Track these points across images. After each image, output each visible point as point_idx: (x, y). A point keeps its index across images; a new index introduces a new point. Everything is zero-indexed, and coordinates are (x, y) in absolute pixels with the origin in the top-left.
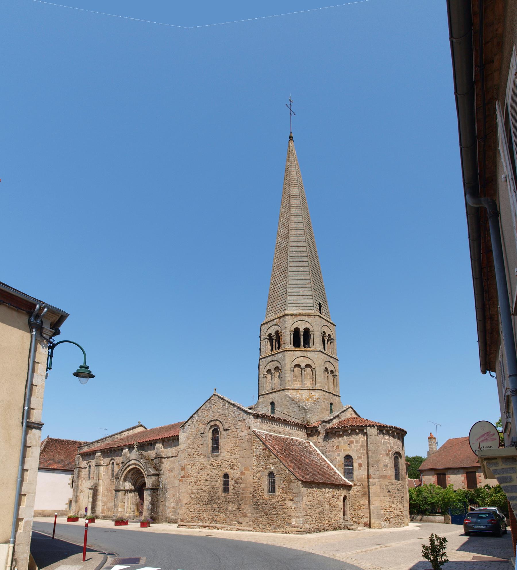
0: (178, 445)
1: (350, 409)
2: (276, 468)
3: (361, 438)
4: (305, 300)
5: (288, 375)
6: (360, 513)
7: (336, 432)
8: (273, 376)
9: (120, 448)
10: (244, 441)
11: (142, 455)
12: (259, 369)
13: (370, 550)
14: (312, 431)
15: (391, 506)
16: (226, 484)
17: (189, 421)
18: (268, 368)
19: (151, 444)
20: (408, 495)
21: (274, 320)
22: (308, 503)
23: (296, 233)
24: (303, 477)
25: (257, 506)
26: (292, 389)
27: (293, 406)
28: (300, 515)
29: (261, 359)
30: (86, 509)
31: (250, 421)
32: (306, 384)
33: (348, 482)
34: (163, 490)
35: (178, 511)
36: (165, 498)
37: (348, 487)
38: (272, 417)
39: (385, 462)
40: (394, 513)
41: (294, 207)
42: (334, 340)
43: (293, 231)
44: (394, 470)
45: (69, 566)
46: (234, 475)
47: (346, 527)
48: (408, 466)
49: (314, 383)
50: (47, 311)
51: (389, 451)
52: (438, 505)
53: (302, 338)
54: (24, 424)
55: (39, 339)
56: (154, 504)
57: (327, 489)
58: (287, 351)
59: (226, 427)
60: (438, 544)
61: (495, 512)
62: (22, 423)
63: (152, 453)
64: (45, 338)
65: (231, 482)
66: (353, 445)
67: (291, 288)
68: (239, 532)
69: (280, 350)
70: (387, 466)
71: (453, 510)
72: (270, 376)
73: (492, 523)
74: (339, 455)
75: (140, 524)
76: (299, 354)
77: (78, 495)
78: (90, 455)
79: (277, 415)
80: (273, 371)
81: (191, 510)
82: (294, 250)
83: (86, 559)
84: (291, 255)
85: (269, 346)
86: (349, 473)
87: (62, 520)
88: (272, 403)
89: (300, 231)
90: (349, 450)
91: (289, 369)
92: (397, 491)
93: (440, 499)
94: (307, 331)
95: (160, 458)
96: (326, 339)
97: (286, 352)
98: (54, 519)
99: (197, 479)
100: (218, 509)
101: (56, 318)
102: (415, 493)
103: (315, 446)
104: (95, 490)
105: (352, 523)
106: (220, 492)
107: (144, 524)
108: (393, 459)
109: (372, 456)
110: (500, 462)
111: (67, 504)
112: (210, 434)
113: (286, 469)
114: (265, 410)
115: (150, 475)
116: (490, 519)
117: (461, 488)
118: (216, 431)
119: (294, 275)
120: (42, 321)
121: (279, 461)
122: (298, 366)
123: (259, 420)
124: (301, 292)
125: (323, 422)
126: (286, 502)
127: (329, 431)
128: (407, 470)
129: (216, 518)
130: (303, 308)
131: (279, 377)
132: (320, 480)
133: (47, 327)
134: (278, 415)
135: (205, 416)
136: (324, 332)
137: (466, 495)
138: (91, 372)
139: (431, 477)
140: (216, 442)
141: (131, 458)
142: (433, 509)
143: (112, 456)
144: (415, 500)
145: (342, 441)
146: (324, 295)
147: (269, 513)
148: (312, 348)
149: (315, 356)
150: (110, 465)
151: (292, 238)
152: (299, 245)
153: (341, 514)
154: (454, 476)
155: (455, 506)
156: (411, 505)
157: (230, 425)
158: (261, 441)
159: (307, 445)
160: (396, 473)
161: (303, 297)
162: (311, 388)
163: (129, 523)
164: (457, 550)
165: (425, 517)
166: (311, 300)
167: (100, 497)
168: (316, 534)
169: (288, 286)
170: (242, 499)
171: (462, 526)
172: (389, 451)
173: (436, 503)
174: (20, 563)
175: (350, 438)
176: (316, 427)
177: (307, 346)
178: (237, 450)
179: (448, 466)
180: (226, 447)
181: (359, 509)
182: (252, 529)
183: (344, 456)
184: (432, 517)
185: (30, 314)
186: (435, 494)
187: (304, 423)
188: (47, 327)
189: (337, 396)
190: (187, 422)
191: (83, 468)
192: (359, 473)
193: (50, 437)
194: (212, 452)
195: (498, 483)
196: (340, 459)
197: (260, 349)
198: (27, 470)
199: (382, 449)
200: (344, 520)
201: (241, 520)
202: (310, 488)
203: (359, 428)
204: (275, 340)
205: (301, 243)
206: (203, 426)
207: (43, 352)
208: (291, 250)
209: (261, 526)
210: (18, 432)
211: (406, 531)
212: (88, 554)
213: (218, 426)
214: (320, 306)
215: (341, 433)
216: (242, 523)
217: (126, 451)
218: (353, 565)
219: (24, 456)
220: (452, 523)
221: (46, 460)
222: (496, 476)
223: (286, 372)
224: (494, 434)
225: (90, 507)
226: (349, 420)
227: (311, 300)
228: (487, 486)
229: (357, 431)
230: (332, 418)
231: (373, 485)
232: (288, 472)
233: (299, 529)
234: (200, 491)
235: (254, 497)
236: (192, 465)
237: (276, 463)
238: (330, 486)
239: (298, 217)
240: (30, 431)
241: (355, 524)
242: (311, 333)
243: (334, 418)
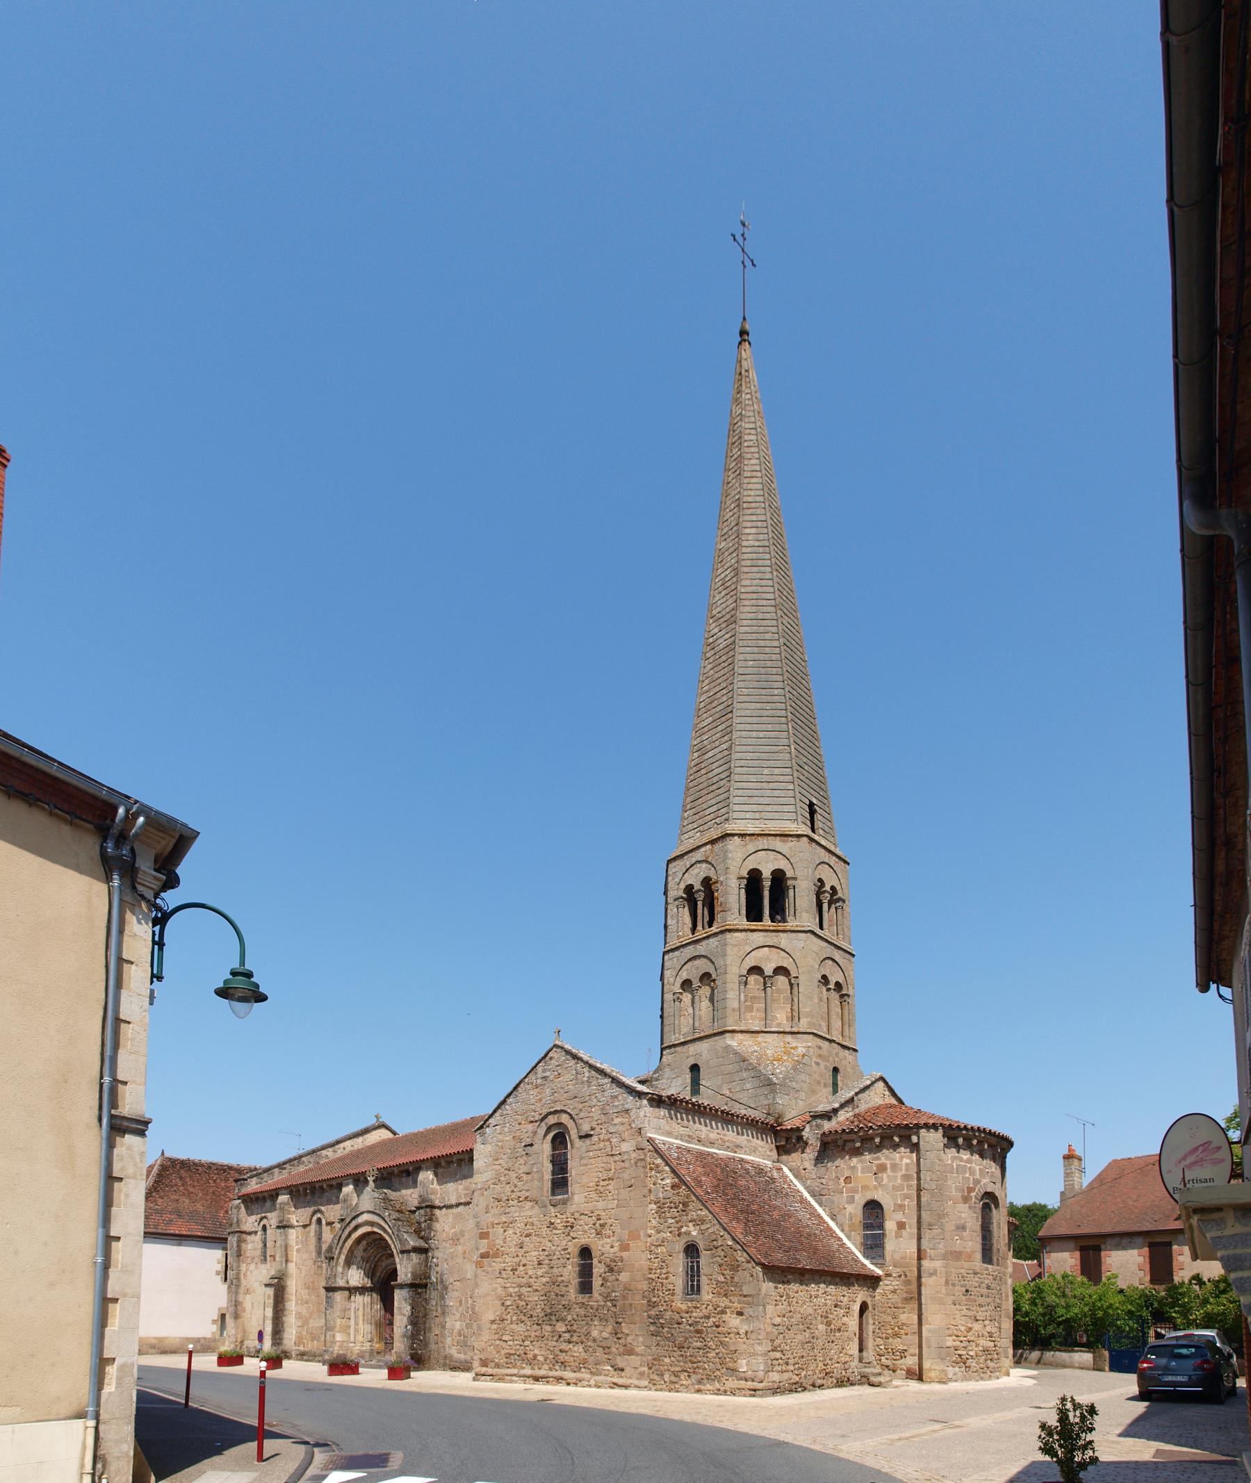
0: (471, 1176)
1: (881, 1084)
2: (702, 1232)
3: (904, 1158)
4: (776, 793)
5: (732, 995)
6: (897, 1344)
7: (845, 1141)
8: (697, 998)
9: (334, 1183)
10: (627, 1164)
11: (386, 1200)
12: (662, 979)
13: (920, 1435)
14: (788, 1139)
15: (971, 1329)
16: (586, 1272)
17: (497, 1114)
18: (684, 975)
19: (408, 1173)
20: (1011, 1300)
21: (699, 847)
22: (778, 1320)
23: (754, 609)
24: (766, 1255)
25: (658, 1326)
26: (742, 1032)
28: (759, 1349)
29: (668, 952)
30: (261, 1335)
31: (642, 1114)
32: (774, 1018)
33: (872, 1267)
34: (439, 1287)
35: (472, 1341)
36: (444, 1306)
37: (872, 1282)
38: (693, 1104)
39: (960, 1217)
40: (977, 1345)
41: (752, 536)
42: (844, 901)
43: (747, 603)
44: (979, 1239)
45: (229, 1473)
46: (604, 1250)
47: (864, 1380)
48: (1012, 1228)
49: (794, 1016)
50: (146, 823)
51: (970, 1190)
52: (1080, 1326)
53: (767, 897)
54: (105, 1121)
55: (128, 898)
56: (418, 1323)
57: (822, 1286)
58: (730, 931)
59: (585, 1128)
60: (1077, 1420)
61: (1210, 1343)
62: (100, 1119)
63: (410, 1196)
64: (142, 896)
65: (598, 1269)
66: (883, 1176)
67: (742, 763)
68: (617, 1392)
69: (714, 929)
70: (963, 1228)
71: (1110, 1337)
72: (690, 996)
73: (1203, 1369)
74: (851, 1200)
75: (386, 1371)
76: (758, 938)
77: (241, 1299)
78: (264, 1199)
79: (704, 1099)
80: (696, 983)
81: (505, 1338)
82: (749, 657)
83: (265, 1456)
84: (741, 671)
85: (687, 919)
86: (874, 1246)
87: (206, 1363)
88: (695, 1068)
89: (764, 603)
90: (875, 1188)
91: (736, 979)
92: (985, 1291)
93: (1086, 1309)
94: (779, 878)
95: (429, 1207)
96: (826, 898)
97: (728, 935)
98: (187, 1358)
99: (517, 1260)
100: (567, 1336)
101: (167, 844)
102: (1028, 1296)
103: (796, 1177)
104: (279, 1288)
105: (878, 1370)
106: (572, 1293)
107: (396, 1372)
108: (979, 1211)
109: (929, 1204)
110: (1230, 1217)
111: (214, 1322)
112: (547, 1147)
113: (727, 1236)
114: (677, 1086)
115: (408, 1252)
116: (1199, 1361)
117: (1137, 1284)
118: (560, 1140)
119: (749, 727)
120: (132, 850)
121: (710, 1217)
122: (756, 970)
123: (663, 1112)
125: (814, 1117)
126: (725, 1317)
127: (829, 1139)
128: (1010, 1239)
129: (562, 1357)
130: (769, 815)
131: (712, 1000)
132: (805, 1262)
133: (145, 866)
134: (708, 1098)
135: (534, 1101)
136: (820, 880)
137: (1147, 1300)
138: (257, 986)
139: (1066, 1255)
140: (560, 1166)
141: (362, 1209)
142: (1069, 1334)
143: (315, 1204)
144: (1027, 1314)
145: (859, 1166)
147: (686, 1345)
148: (791, 923)
150: (313, 1226)
151: (745, 623)
152: (762, 643)
153: (853, 1348)
154: (1120, 1253)
155: (1118, 1328)
156: (1016, 1324)
157: (594, 1124)
158: (667, 1164)
159: (775, 1174)
160: (984, 1245)
161: (771, 786)
162: (788, 1030)
163: (361, 1370)
164: (1120, 1435)
165: (1049, 1355)
166: (791, 793)
167: (292, 1305)
168: (796, 1395)
169: (735, 756)
170: (623, 1310)
171: (1133, 1378)
172: (970, 1190)
173: (1075, 1321)
174: (113, 1467)
175: (878, 1158)
176: (799, 1130)
177: (779, 917)
178: (610, 1187)
179: (1108, 1229)
180: (585, 1179)
181: (896, 1335)
182: (646, 1383)
183: (863, 1202)
184: (1064, 1354)
185: (103, 831)
186: (1075, 1297)
187: (771, 1120)
188: (145, 866)
189: (849, 1048)
190: (491, 1116)
191: (250, 1233)
192: (899, 1246)
193: (167, 1155)
194: (553, 1194)
195: (1222, 1272)
196: (854, 1210)
197: (666, 927)
198: (118, 1239)
199: (954, 1186)
200: (860, 1361)
201: (620, 1362)
202: (783, 1283)
203: (899, 1133)
204: (702, 901)
205: (768, 636)
206: (530, 1127)
207: (139, 932)
208: (741, 657)
209: (666, 1377)
210: (90, 1139)
211: (1003, 1389)
212: (270, 1445)
213: (566, 1127)
214: (812, 812)
215: (858, 1145)
216: (622, 1370)
217: (349, 1189)
218: (879, 1472)
219: (108, 1202)
220: (1111, 1370)
221: (160, 1212)
222: (1219, 1254)
223: (729, 986)
224: (1219, 1148)
225: (268, 1330)
226: (876, 1110)
227: (791, 793)
228: (1197, 1278)
229: (896, 1139)
230: (836, 1105)
231: (931, 1275)
232: (730, 1243)
233: (756, 1385)
234: (524, 1290)
235: (652, 1305)
236: (506, 1226)
237: (703, 1221)
238: (829, 1279)
239: (760, 563)
240: (118, 1139)
241: (886, 1372)
242: (789, 882)
243: (842, 1106)
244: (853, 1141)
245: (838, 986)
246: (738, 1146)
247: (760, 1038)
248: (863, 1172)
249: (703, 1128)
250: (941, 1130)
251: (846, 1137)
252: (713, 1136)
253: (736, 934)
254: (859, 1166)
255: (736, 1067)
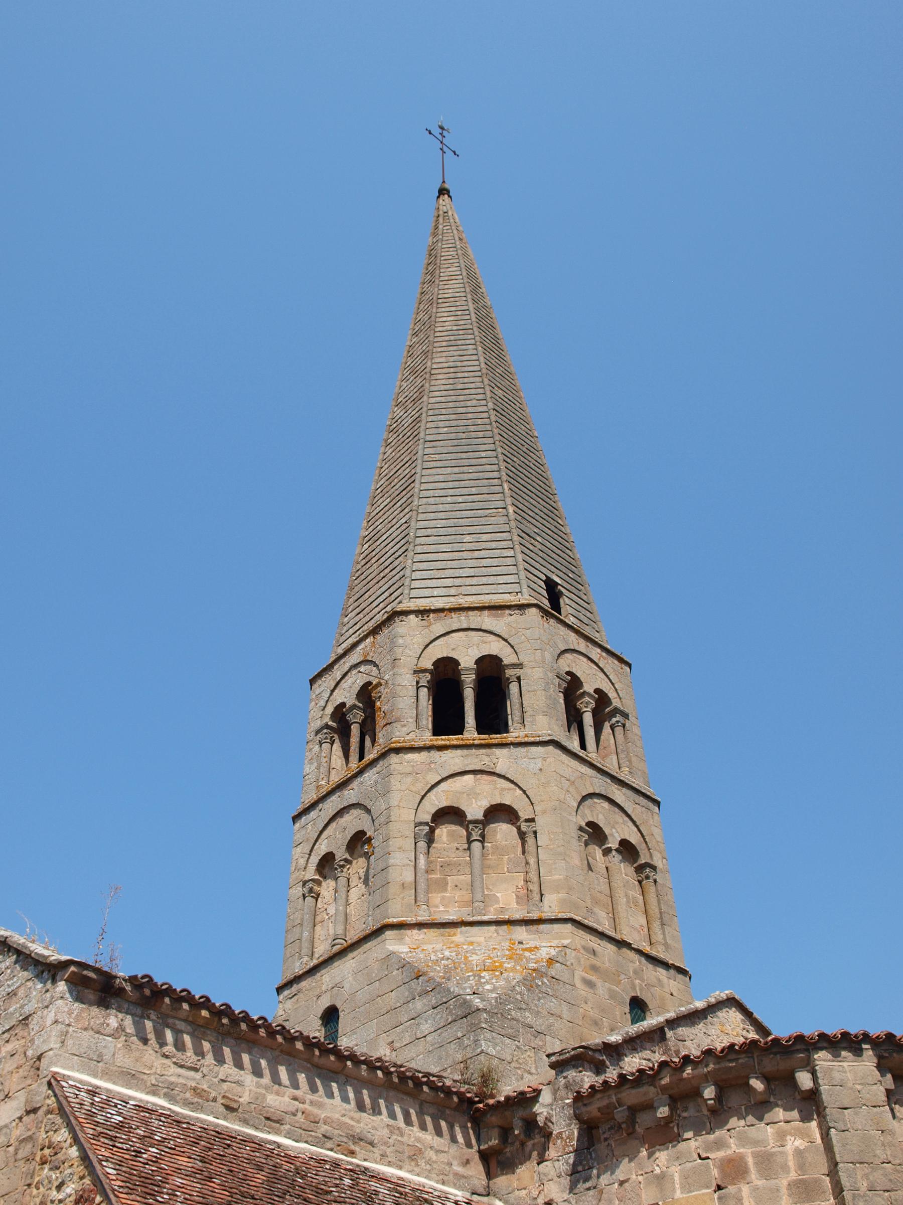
3: (785, 1136)
5: (399, 855)
7: (634, 1111)
14: (505, 1132)
18: (323, 848)
26: (420, 925)
27: (419, 1005)
42: (626, 716)
49: (534, 890)
76: (454, 760)
122: (450, 814)
124: (467, 538)
127: (592, 1110)
145: (675, 1172)
146: (563, 544)
149: (535, 771)
162: (517, 916)
175: (719, 1145)
176: (525, 1100)
215: (663, 1112)
223: (394, 844)
229: (757, 1084)
244: (650, 1107)
245: (627, 850)
246: (358, 1139)
247: (460, 935)
248: (687, 1187)
249: (249, 1079)
250: (869, 1053)
251: (632, 1096)
252: (278, 1101)
253: (410, 756)
254: (675, 1172)
255: (404, 992)
